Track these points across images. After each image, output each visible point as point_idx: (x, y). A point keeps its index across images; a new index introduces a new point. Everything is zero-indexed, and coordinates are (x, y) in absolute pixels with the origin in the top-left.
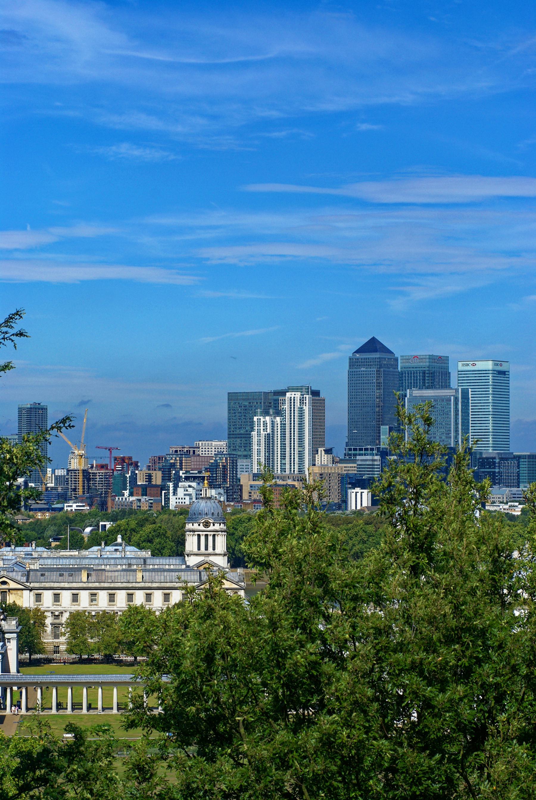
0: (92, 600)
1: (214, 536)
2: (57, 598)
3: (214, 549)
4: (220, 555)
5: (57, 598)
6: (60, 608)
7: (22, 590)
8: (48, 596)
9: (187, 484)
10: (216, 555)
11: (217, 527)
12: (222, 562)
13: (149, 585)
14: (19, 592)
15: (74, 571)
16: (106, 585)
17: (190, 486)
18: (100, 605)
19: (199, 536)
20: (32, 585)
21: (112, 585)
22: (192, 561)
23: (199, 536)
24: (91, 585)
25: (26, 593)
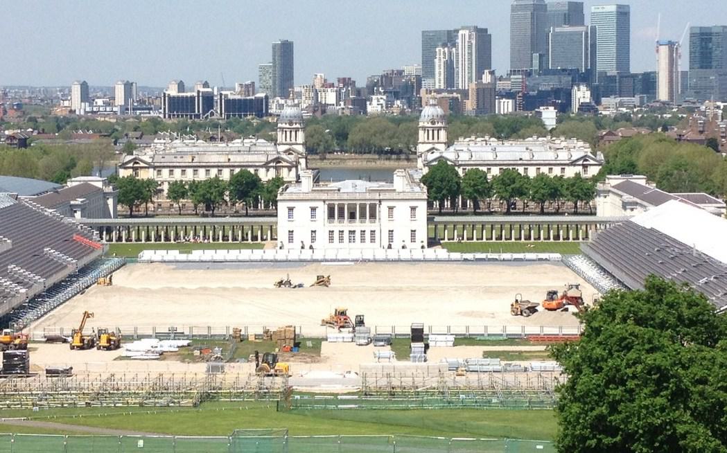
0: (194, 174)
1: (296, 132)
3: (296, 140)
4: (300, 144)
7: (148, 168)
8: (165, 172)
9: (379, 97)
10: (297, 144)
11: (298, 126)
12: (300, 149)
13: (233, 164)
15: (182, 154)
16: (204, 164)
17: (381, 98)
18: (188, 177)
19: (286, 131)
20: (156, 164)
21: (208, 164)
22: (282, 148)
23: (286, 131)
24: (194, 164)
25: (151, 170)
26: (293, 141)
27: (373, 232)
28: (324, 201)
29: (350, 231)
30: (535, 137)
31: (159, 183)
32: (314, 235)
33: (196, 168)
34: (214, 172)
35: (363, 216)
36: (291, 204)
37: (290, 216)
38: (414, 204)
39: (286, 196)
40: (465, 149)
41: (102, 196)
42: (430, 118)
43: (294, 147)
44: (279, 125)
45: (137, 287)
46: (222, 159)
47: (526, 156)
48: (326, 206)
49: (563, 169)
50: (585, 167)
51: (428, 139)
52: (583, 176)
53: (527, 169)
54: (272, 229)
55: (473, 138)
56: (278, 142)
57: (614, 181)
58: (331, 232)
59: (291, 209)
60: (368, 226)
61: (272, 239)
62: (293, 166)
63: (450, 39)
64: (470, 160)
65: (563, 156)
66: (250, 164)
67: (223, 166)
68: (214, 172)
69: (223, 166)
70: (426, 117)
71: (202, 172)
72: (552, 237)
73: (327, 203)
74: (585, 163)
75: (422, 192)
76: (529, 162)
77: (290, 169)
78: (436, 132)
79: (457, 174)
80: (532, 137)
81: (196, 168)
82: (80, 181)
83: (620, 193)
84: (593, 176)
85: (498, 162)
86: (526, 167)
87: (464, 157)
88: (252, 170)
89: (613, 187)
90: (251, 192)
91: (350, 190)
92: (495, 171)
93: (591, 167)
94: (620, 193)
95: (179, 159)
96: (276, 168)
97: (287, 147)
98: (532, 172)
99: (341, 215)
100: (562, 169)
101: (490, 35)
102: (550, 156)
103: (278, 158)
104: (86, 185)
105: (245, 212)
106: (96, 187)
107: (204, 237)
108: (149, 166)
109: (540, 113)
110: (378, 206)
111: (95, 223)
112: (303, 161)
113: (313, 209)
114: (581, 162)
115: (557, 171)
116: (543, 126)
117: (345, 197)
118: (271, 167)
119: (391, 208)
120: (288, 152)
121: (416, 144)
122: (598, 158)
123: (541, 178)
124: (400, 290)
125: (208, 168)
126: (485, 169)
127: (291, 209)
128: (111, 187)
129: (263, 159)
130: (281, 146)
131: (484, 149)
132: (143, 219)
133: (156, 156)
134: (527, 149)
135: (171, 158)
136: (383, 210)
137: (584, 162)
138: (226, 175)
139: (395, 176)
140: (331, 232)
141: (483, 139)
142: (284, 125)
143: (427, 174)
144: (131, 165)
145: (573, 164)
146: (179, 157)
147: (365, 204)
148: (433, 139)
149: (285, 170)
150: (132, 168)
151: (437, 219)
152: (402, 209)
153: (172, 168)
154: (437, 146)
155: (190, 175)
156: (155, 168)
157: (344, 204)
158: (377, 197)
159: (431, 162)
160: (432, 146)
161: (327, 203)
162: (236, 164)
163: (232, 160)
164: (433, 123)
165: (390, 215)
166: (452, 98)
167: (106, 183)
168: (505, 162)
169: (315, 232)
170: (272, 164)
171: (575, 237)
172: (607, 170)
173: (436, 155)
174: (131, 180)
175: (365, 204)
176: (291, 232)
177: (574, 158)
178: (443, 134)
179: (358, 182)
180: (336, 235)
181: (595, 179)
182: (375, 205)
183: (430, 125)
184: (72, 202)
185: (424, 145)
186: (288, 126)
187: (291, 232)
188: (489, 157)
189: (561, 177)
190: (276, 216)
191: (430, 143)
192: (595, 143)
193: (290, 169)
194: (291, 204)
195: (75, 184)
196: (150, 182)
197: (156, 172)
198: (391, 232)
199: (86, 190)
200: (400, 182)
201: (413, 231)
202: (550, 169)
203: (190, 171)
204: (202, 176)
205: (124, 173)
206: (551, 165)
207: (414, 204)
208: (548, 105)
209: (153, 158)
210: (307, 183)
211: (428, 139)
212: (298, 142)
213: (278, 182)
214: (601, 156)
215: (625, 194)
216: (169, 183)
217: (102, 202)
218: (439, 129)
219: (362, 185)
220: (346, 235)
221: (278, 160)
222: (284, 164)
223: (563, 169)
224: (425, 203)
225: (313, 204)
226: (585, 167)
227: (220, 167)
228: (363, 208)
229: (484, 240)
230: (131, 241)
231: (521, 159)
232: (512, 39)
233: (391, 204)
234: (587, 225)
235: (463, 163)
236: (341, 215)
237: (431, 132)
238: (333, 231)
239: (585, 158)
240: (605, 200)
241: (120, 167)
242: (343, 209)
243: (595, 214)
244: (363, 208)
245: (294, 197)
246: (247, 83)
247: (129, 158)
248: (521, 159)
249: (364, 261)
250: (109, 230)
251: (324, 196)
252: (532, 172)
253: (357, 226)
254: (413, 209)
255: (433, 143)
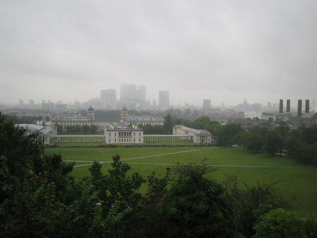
35: (128, 135)
36: (110, 132)
46: (77, 120)
59: (110, 134)
65: (158, 120)
87: (136, 120)
102: (155, 120)
113: (115, 134)
115: (157, 124)
119: (134, 134)
125: (74, 122)
127: (110, 134)
129: (88, 120)
135: (64, 120)
176: (110, 139)
187: (110, 139)
254: (140, 133)
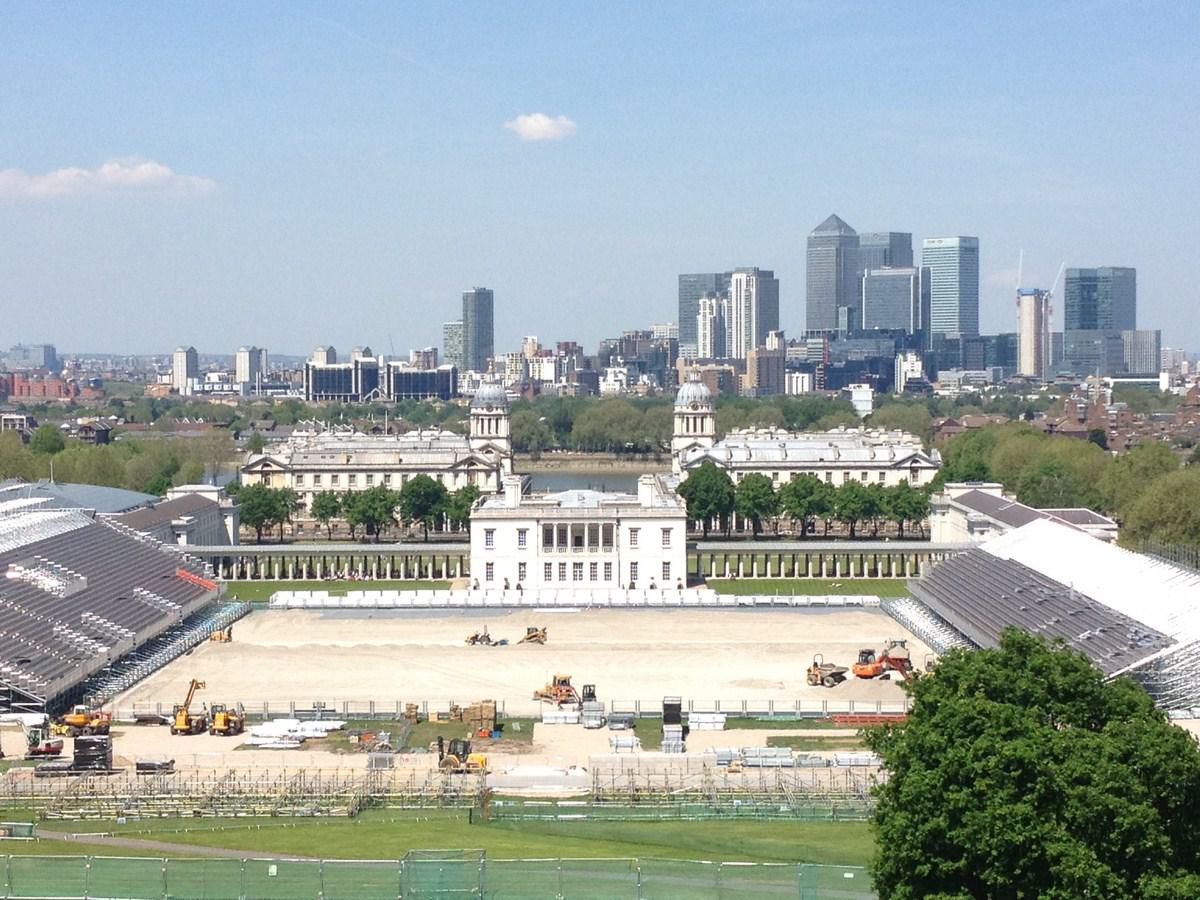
0: (350, 482)
1: (497, 420)
2: (317, 479)
5: (317, 479)
6: (301, 489)
7: (284, 472)
8: (309, 478)
9: (617, 370)
10: (499, 438)
11: (500, 412)
12: (503, 445)
13: (406, 467)
14: (282, 475)
15: (333, 452)
16: (364, 467)
17: (620, 372)
18: (342, 486)
19: (482, 420)
21: (371, 467)
22: (476, 444)
23: (482, 420)
25: (288, 475)
26: (494, 434)
27: (608, 565)
28: (538, 520)
29: (575, 564)
30: (842, 428)
31: (300, 494)
32: (523, 569)
33: (352, 473)
34: (378, 478)
35: (593, 541)
36: (490, 525)
37: (489, 542)
38: (667, 524)
39: (482, 513)
40: (741, 445)
41: (217, 512)
42: (690, 400)
43: (493, 441)
44: (473, 411)
45: (268, 644)
46: (391, 460)
47: (830, 456)
48: (541, 528)
49: (882, 474)
50: (914, 470)
51: (688, 430)
52: (912, 484)
53: (830, 473)
54: (463, 561)
55: (752, 429)
56: (472, 435)
57: (956, 491)
58: (548, 565)
59: (490, 532)
60: (601, 556)
61: (462, 575)
62: (493, 470)
63: (719, 286)
64: (748, 460)
65: (883, 455)
66: (432, 467)
67: (391, 470)
68: (378, 478)
69: (391, 470)
70: (685, 399)
71: (361, 478)
72: (866, 572)
73: (542, 522)
74: (914, 465)
75: (679, 507)
76: (834, 464)
77: (488, 474)
78: (699, 421)
79: (729, 481)
80: (837, 427)
81: (352, 473)
82: (186, 492)
83: (964, 508)
84: (926, 484)
85: (788, 464)
86: (829, 471)
87: (740, 456)
88: (433, 476)
89: (955, 500)
90: (433, 507)
91: (576, 504)
92: (785, 477)
93: (923, 471)
94: (964, 508)
95: (328, 460)
96: (468, 472)
97: (484, 442)
98: (838, 480)
99: (562, 541)
100: (881, 473)
101: (777, 281)
102: (863, 455)
103: (472, 458)
104: (194, 496)
105: (423, 536)
106: (209, 500)
107: (365, 572)
108: (286, 470)
109: (849, 393)
110: (615, 527)
111: (208, 552)
112: (507, 463)
113: (522, 532)
114: (908, 464)
115: (873, 477)
116: (854, 411)
117: (568, 514)
118: (461, 471)
119: (634, 531)
120: (486, 449)
121: (670, 438)
122: (933, 458)
123: (851, 486)
124: (647, 648)
125: (370, 472)
126: (769, 474)
127: (490, 532)
128: (230, 500)
129: (450, 459)
130: (476, 441)
131: (768, 445)
132: (277, 546)
133: (295, 455)
134: (831, 445)
135: (317, 459)
136: (622, 533)
137: (913, 464)
138: (396, 483)
139: (640, 484)
140: (548, 565)
141: (767, 431)
142: (479, 411)
143: (686, 481)
144: (259, 468)
145: (897, 466)
146: (328, 456)
147: (597, 525)
148: (695, 430)
149: (482, 475)
150: (261, 472)
151: (701, 546)
152: (650, 531)
153: (317, 473)
154: (700, 441)
155: (344, 483)
156: (293, 472)
157: (566, 525)
158: (614, 514)
159: (692, 463)
160: (692, 442)
161: (542, 522)
162: (411, 467)
163: (404, 462)
164: (695, 407)
165: (633, 541)
166: (723, 372)
167: (222, 495)
168: (799, 464)
169: (524, 564)
170: (462, 467)
171: (900, 572)
172: (947, 476)
173: (700, 453)
174: (259, 490)
175: (597, 525)
176: (490, 565)
177: (898, 458)
178: (709, 423)
179: (587, 493)
180: (555, 570)
181: (929, 489)
182: (612, 526)
183: (690, 410)
184: (174, 522)
185: (682, 439)
186: (485, 412)
187: (490, 565)
188: (776, 456)
189: (880, 485)
190: (469, 542)
191: (690, 436)
192: (929, 436)
193: (488, 474)
194: (490, 525)
195: (178, 495)
196: (287, 493)
197: (294, 478)
198: (634, 564)
199: (194, 505)
200: (646, 493)
201: (666, 564)
202: (863, 473)
203: (344, 478)
204: (361, 483)
205: (249, 480)
206: (864, 469)
207: (667, 524)
208: (860, 381)
209: (290, 458)
210: (513, 494)
211: (688, 430)
212: (500, 435)
213: (471, 493)
214: (937, 456)
215: (972, 510)
216: (314, 494)
217: (218, 521)
218: (703, 416)
219: (593, 497)
220: (569, 569)
221: (471, 461)
222: (480, 466)
223: (882, 474)
224: (683, 524)
225: (522, 525)
226: (914, 470)
227: (388, 472)
228: (593, 530)
229: (769, 577)
230: (259, 577)
231: (821, 460)
232: (809, 285)
233: (634, 524)
234: (916, 555)
235: (739, 465)
236: (562, 541)
237: (691, 421)
238: (550, 564)
239: (914, 458)
240: (944, 518)
241: (244, 471)
242: (565, 531)
243: (929, 539)
244: (593, 530)
245: (495, 514)
246: (426, 349)
247: (257, 458)
248: (821, 460)
249: (596, 606)
250: (227, 563)
251: (538, 514)
252: (838, 480)
253: (586, 556)
254: (666, 531)
255: (696, 437)
